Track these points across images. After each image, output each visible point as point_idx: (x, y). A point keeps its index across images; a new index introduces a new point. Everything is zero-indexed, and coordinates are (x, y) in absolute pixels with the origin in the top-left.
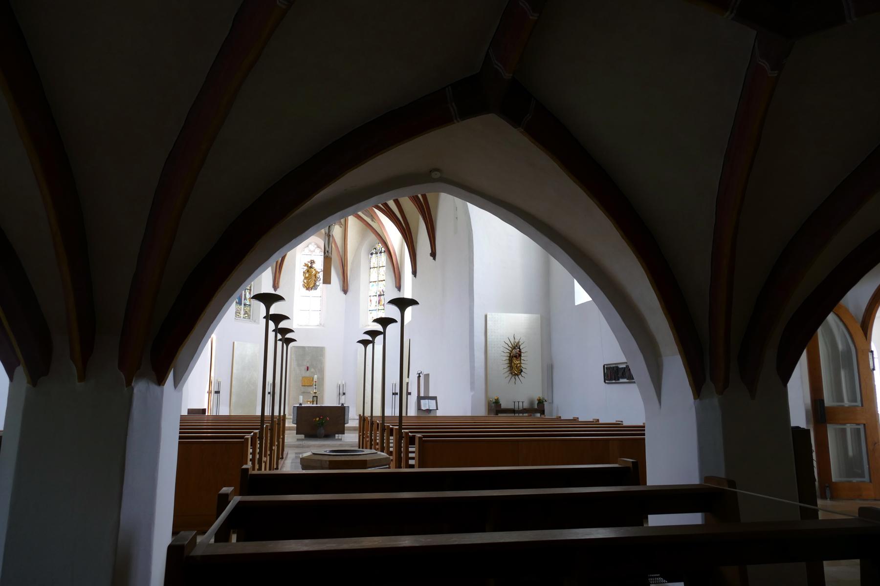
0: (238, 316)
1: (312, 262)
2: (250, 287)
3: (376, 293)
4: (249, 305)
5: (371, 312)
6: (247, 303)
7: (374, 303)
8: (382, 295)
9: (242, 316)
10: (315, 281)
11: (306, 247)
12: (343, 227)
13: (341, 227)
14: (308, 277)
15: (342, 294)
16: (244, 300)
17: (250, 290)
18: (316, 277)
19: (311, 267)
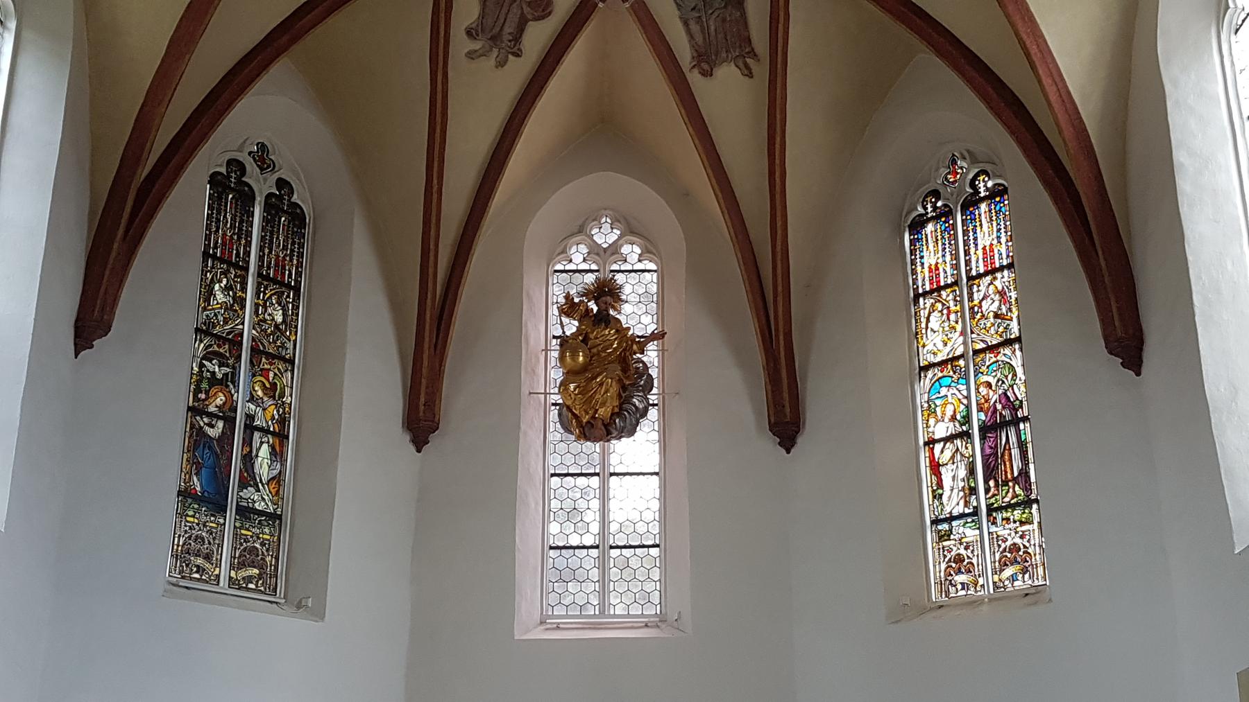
0: (200, 569)
1: (607, 292)
2: (283, 421)
3: (967, 419)
4: (275, 518)
5: (944, 527)
6: (260, 506)
7: (953, 475)
8: (1004, 424)
9: (224, 571)
10: (624, 388)
11: (572, 235)
12: (761, 70)
13: (750, 75)
14: (585, 368)
15: (769, 445)
16: (243, 485)
17: (282, 436)
18: (625, 370)
19: (603, 319)
